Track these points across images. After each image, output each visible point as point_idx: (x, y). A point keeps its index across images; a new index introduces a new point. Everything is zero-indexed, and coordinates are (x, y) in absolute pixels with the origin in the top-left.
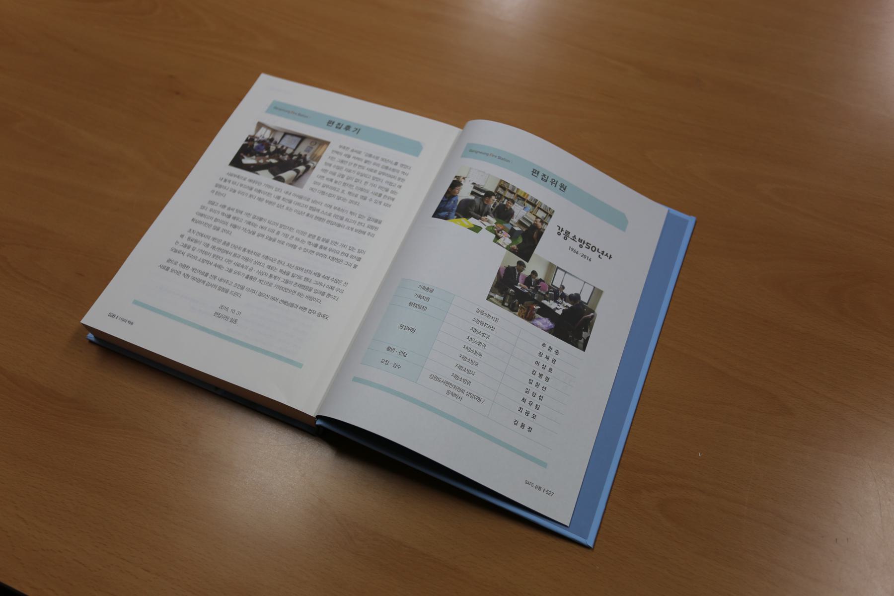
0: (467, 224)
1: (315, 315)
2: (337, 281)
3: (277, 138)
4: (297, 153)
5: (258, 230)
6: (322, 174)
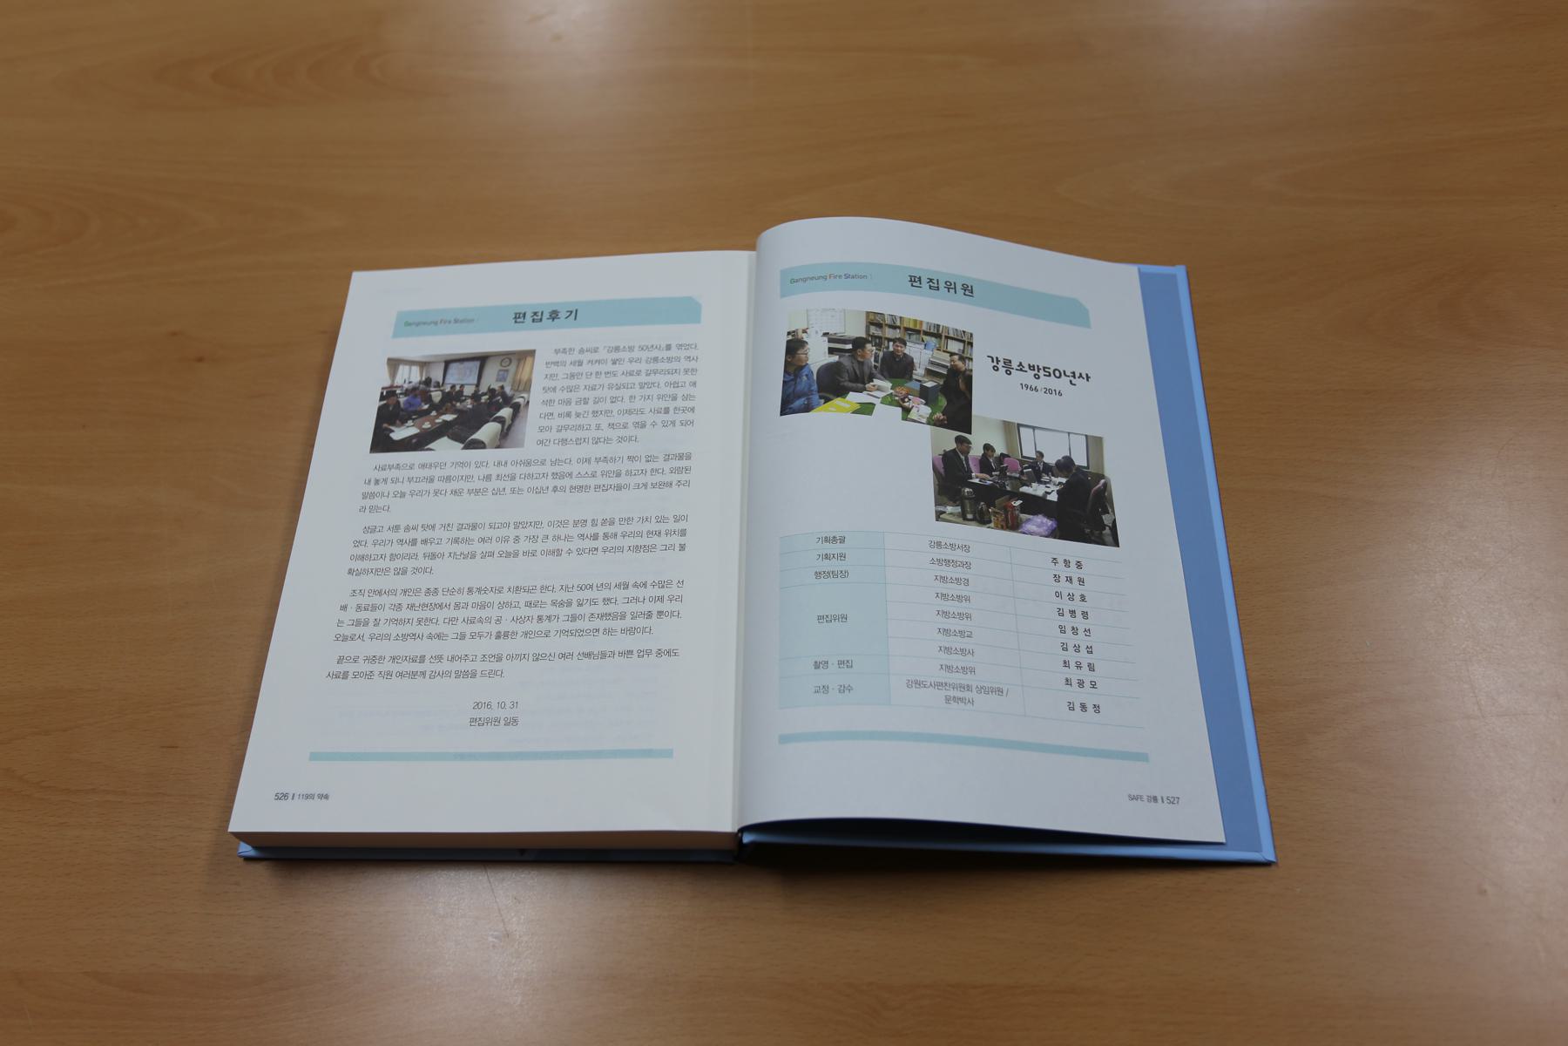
0: (847, 406)
1: (653, 657)
2: (662, 585)
3: (437, 374)
4: (484, 389)
5: (479, 548)
6: (548, 409)
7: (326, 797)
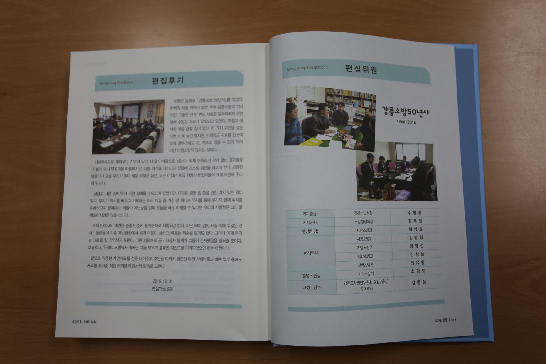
0: (316, 142)
1: (230, 261)
2: (233, 226)
3: (119, 112)
4: (142, 121)
5: (148, 204)
6: (173, 133)
7: (95, 322)
